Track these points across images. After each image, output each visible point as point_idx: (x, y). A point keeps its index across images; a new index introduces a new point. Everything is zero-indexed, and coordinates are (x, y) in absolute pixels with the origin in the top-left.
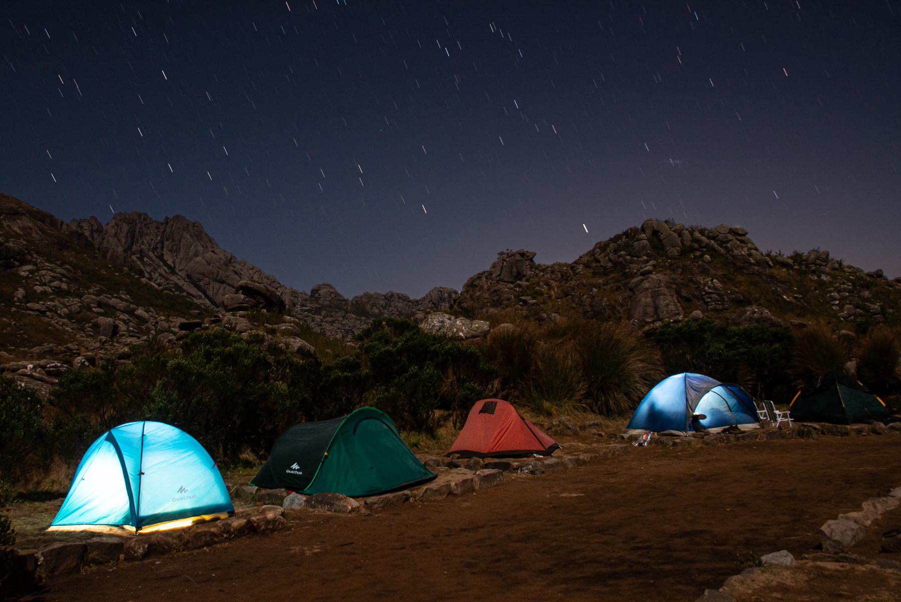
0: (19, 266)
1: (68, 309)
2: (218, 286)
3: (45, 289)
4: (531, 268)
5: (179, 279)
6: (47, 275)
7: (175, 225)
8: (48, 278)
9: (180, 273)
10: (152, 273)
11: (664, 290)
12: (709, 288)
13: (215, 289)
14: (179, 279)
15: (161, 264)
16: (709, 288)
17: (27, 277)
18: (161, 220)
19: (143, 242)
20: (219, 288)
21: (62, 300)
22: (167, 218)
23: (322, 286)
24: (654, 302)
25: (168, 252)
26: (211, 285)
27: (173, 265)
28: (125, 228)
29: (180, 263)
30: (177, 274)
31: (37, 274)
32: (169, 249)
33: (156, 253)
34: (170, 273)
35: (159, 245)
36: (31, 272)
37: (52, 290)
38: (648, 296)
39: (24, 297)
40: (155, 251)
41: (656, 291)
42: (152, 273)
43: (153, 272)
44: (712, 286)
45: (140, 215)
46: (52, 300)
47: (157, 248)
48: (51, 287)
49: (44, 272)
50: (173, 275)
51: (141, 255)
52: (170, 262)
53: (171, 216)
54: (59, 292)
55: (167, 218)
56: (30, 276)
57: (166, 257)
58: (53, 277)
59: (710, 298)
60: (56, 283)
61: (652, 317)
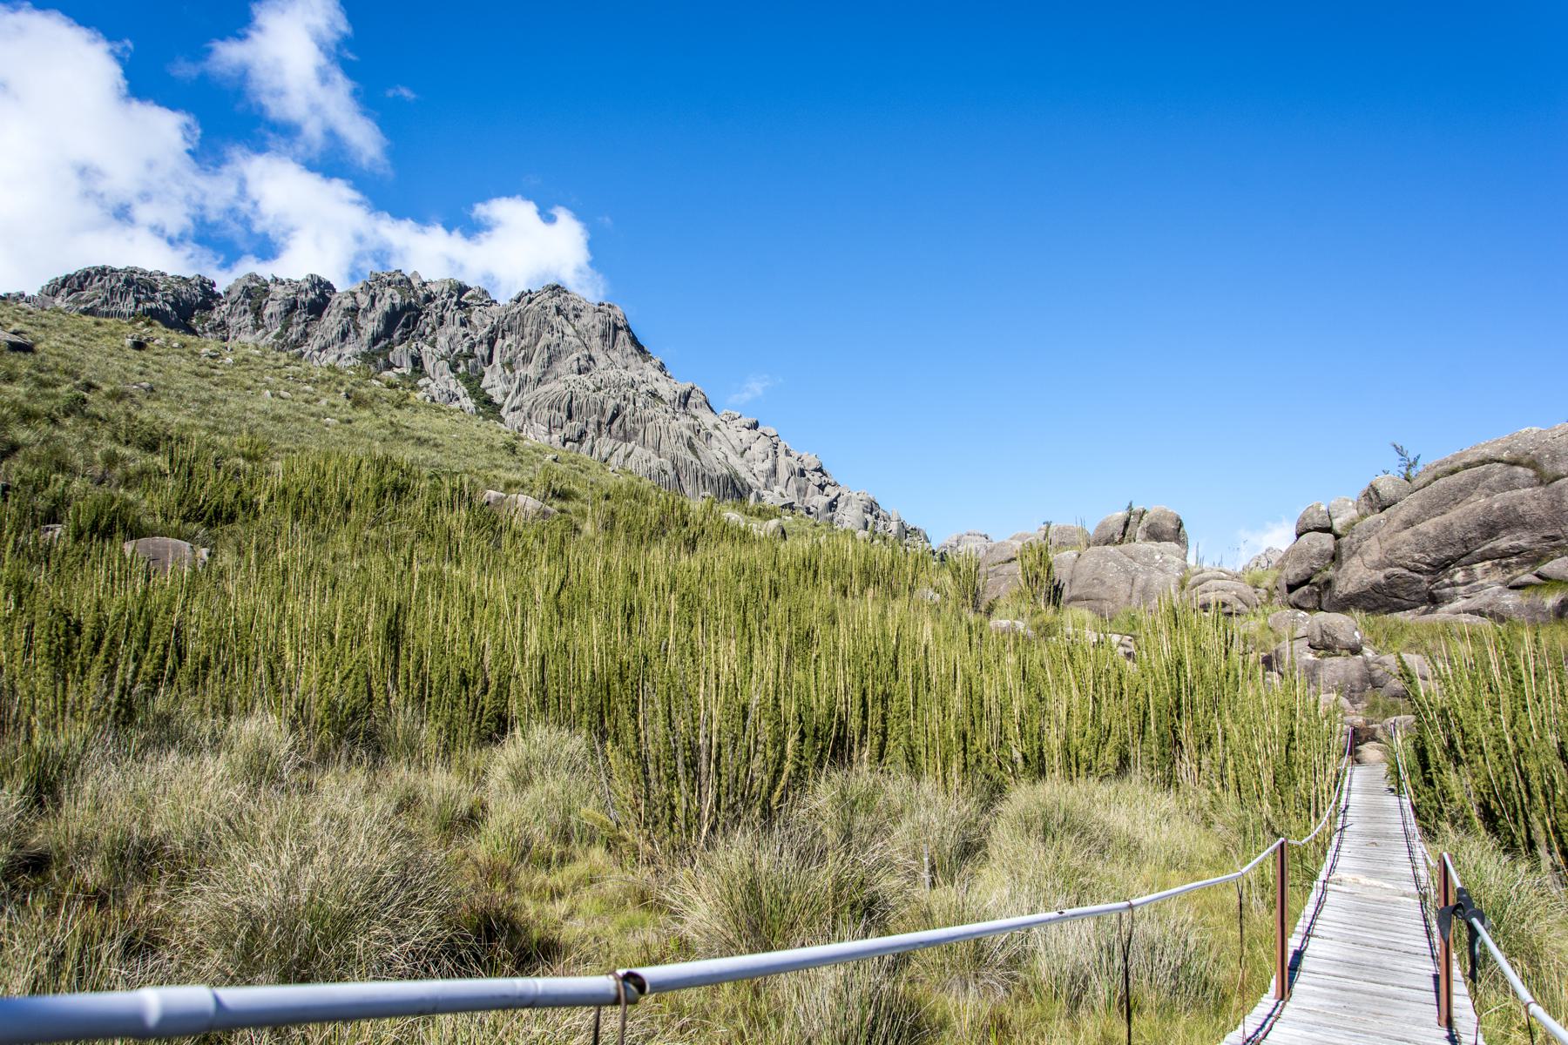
2: (606, 450)
9: (508, 418)
13: (596, 455)
15: (461, 390)
19: (435, 340)
20: (611, 454)
23: (966, 537)
25: (499, 369)
26: (587, 445)
27: (498, 399)
30: (501, 419)
32: (506, 360)
33: (462, 369)
34: (479, 414)
40: (461, 362)
45: (462, 289)
51: (414, 371)
57: (485, 383)
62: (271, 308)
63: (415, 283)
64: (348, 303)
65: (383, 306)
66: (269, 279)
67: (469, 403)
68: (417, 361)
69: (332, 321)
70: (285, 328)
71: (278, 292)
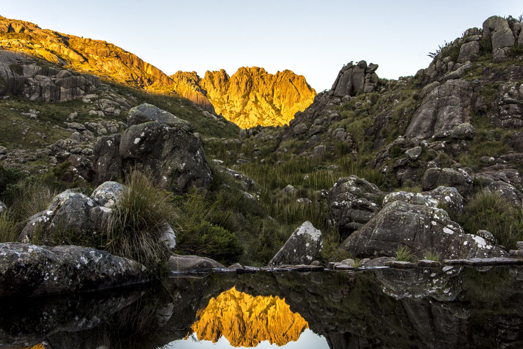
0: (85, 95)
1: (107, 129)
3: (98, 113)
4: (371, 81)
5: (283, 119)
6: (105, 102)
7: (283, 77)
8: (105, 105)
10: (263, 114)
11: (455, 98)
12: (511, 95)
14: (283, 119)
15: (270, 107)
16: (511, 95)
17: (89, 104)
18: (274, 73)
19: (258, 90)
21: (105, 122)
22: (279, 72)
24: (435, 113)
28: (245, 78)
29: (284, 107)
30: (282, 116)
31: (97, 101)
32: (278, 96)
35: (271, 92)
36: (93, 100)
37: (105, 114)
38: (432, 106)
39: (75, 118)
41: (444, 100)
42: (263, 114)
43: (264, 113)
44: (516, 92)
45: (258, 69)
46: (96, 122)
47: (269, 95)
48: (104, 112)
49: (103, 100)
50: (279, 116)
51: (256, 100)
52: (277, 106)
53: (281, 71)
54: (110, 116)
55: (279, 72)
56: (91, 102)
57: (274, 103)
58: (109, 104)
59: (507, 109)
60: (108, 109)
61: (425, 132)
62: (216, 82)
63: (248, 70)
64: (236, 81)
65: (244, 81)
66: (212, 71)
67: (273, 111)
68: (256, 97)
69: (233, 86)
70: (221, 87)
71: (215, 75)
